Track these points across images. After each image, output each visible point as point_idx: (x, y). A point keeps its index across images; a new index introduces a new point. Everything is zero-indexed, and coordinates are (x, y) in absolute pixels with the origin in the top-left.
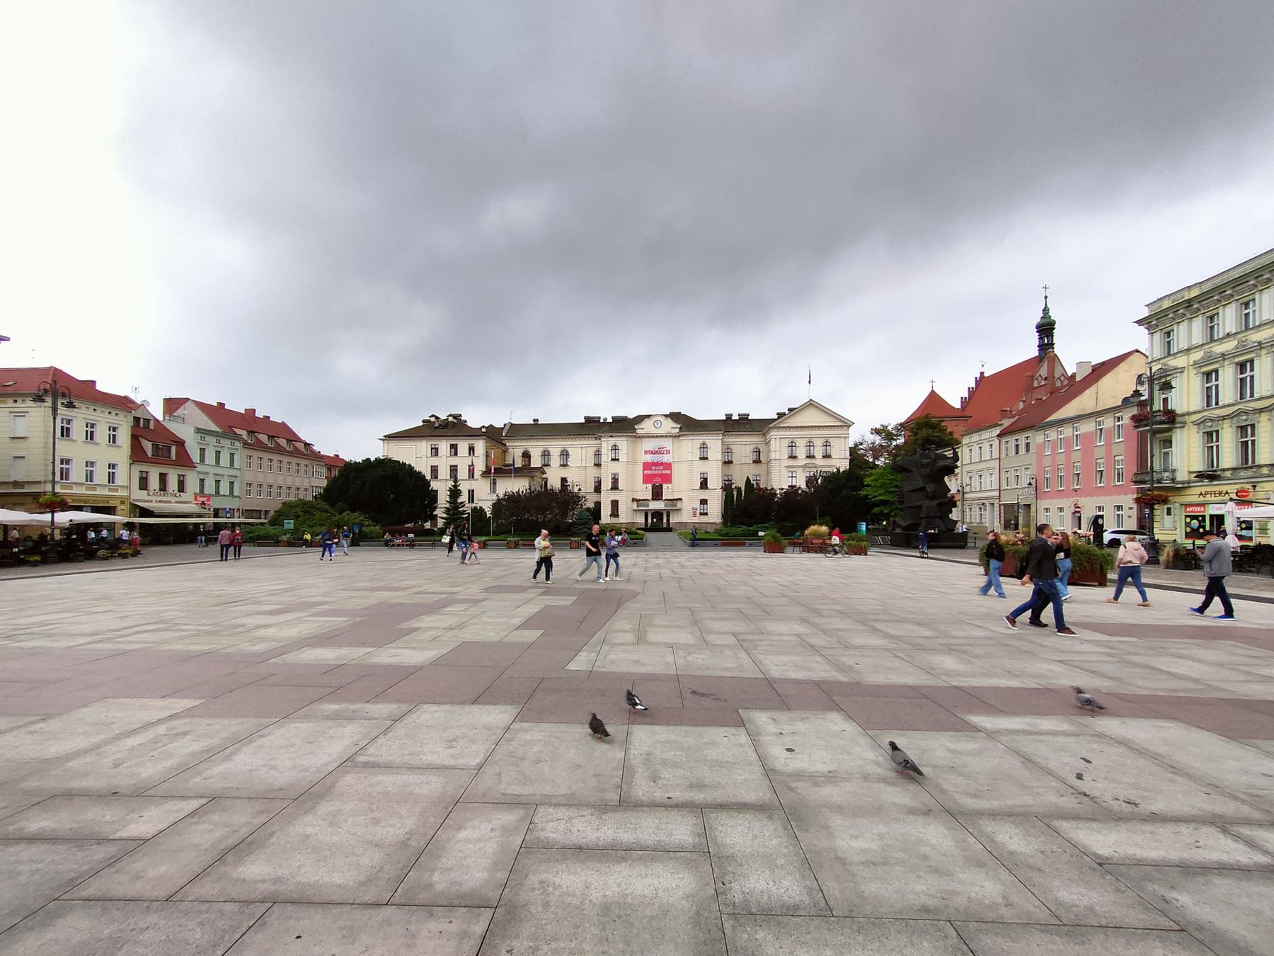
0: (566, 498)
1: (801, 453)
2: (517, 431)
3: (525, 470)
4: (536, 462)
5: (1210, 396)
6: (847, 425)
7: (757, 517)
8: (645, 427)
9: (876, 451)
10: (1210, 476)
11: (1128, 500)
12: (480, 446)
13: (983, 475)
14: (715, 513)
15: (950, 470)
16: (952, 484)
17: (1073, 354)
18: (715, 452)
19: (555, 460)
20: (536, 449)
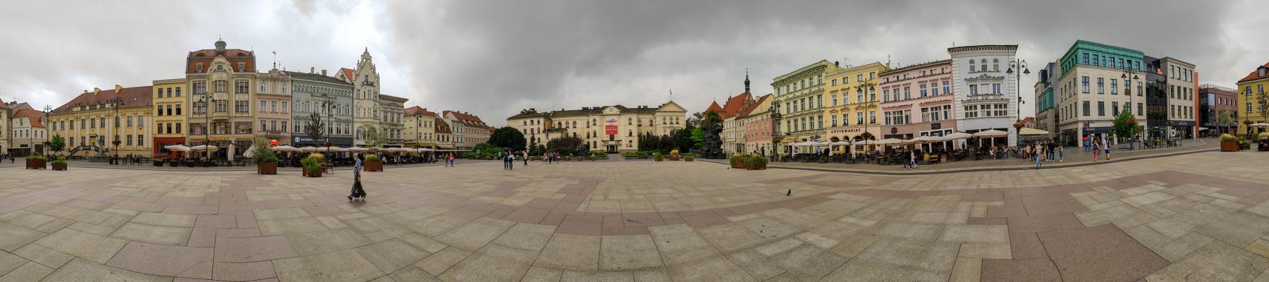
0: (576, 140)
1: (668, 121)
2: (556, 114)
3: (560, 130)
4: (564, 126)
5: (788, 109)
6: (685, 111)
7: (651, 147)
8: (606, 111)
9: (696, 122)
10: (789, 134)
11: (770, 142)
12: (542, 120)
13: (731, 131)
14: (635, 146)
15: (720, 131)
16: (721, 136)
17: (756, 93)
18: (635, 122)
19: (571, 125)
20: (563, 121)
